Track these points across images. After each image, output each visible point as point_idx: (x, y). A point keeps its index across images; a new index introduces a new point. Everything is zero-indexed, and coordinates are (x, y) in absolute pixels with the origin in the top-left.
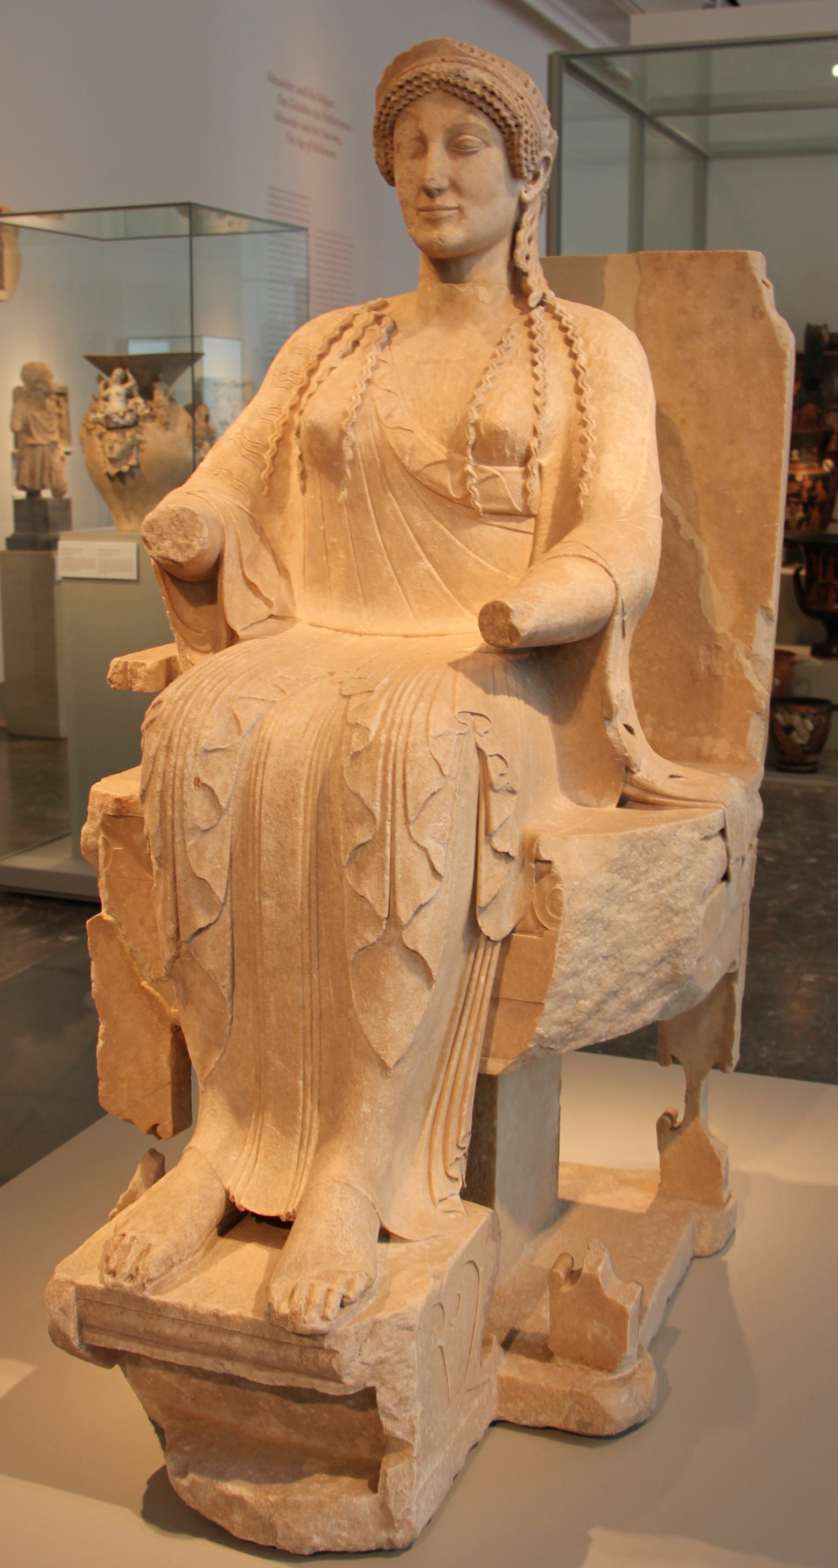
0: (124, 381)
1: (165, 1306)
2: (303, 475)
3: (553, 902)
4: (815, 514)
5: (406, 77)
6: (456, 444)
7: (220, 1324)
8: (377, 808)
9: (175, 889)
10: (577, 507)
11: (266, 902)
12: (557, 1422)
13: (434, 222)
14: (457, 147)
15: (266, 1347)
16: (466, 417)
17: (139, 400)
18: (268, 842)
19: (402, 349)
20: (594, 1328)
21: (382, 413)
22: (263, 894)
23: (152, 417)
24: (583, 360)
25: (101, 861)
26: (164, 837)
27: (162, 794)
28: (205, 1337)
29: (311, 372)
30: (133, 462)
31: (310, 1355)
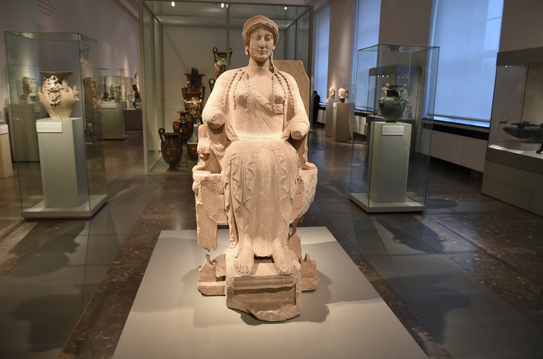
0: (54, 79)
1: (256, 277)
2: (235, 106)
3: (303, 188)
4: (198, 112)
5: (256, 23)
6: (270, 99)
7: (269, 278)
8: (287, 171)
9: (243, 192)
10: (294, 112)
11: (262, 193)
12: (306, 290)
13: (262, 54)
14: (267, 39)
15: (278, 280)
16: (273, 94)
17: (59, 84)
18: (263, 180)
19: (251, 80)
20: (310, 270)
21: (254, 93)
22: (261, 191)
23: (62, 89)
24: (289, 83)
25: (199, 191)
26: (241, 182)
27: (241, 173)
28: (264, 281)
29: (231, 84)
30: (59, 101)
31: (288, 279)
